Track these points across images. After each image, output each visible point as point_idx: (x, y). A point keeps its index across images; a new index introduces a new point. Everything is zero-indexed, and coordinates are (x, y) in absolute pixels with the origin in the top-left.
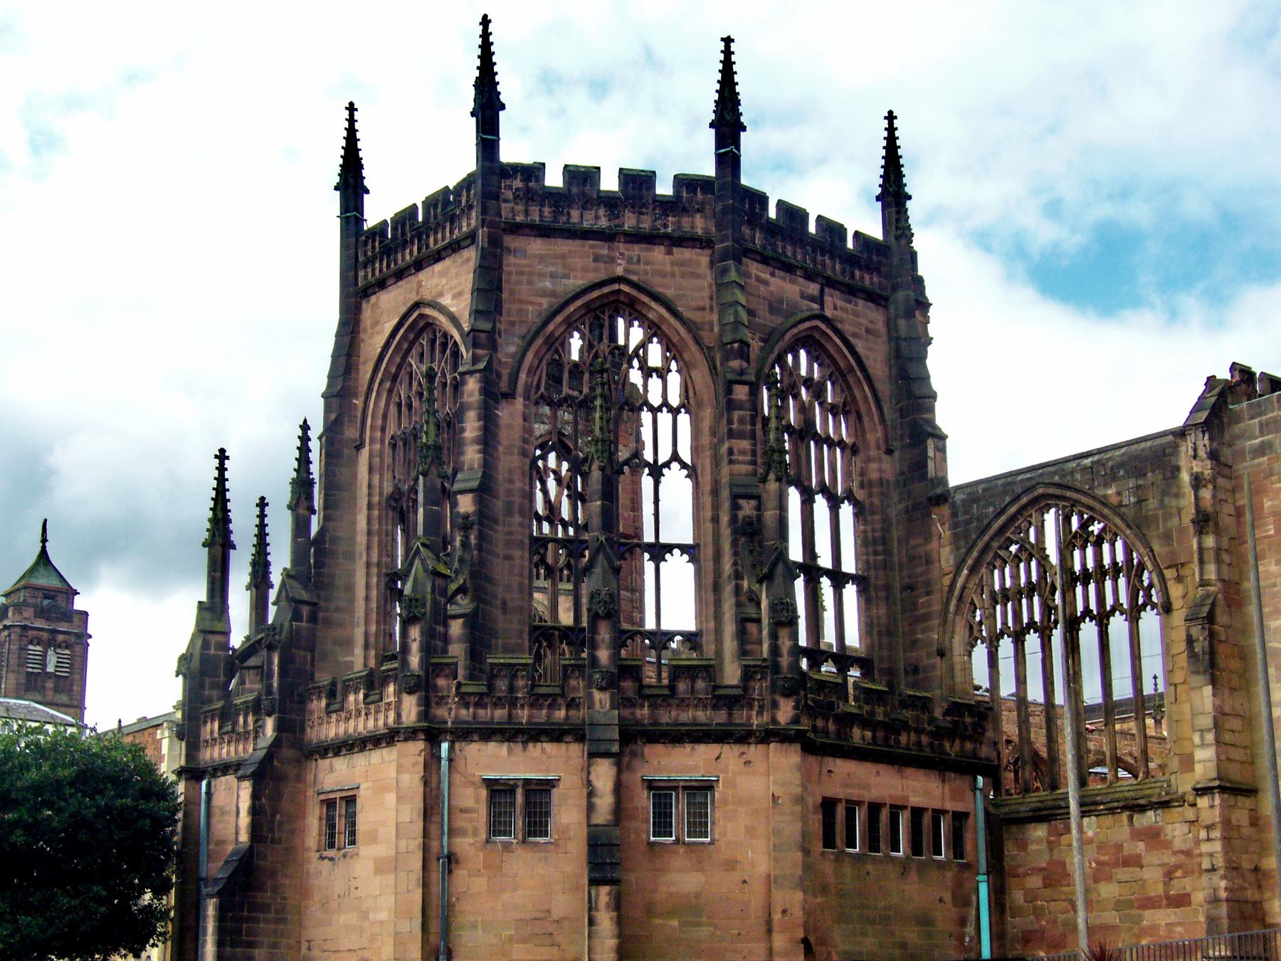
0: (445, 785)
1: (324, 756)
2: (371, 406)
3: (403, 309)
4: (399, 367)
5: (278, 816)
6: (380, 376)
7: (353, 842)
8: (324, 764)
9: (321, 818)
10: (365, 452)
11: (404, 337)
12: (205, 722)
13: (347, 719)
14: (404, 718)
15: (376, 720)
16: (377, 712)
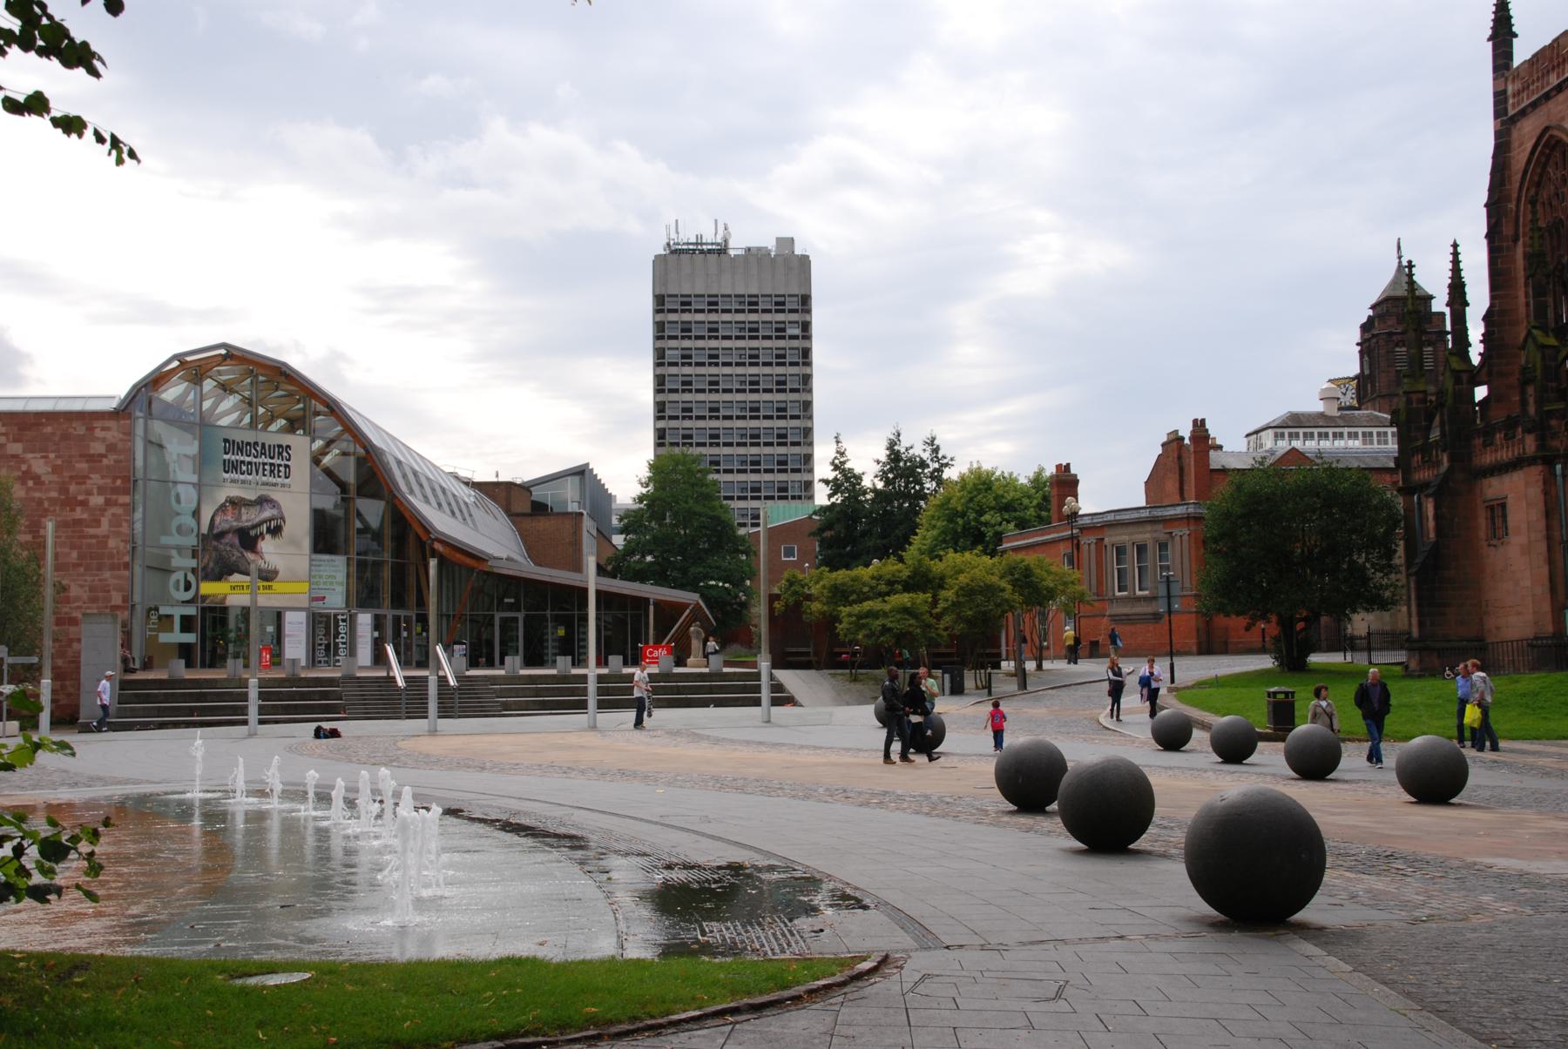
0: (1561, 494)
1: (1485, 477)
2: (1522, 208)
3: (1538, 132)
4: (1541, 175)
5: (1456, 520)
6: (1526, 184)
7: (1507, 534)
8: (1486, 482)
9: (1486, 519)
10: (1520, 243)
11: (1542, 153)
12: (1413, 456)
13: (1496, 451)
14: (1527, 450)
15: (1513, 451)
16: (1513, 446)
